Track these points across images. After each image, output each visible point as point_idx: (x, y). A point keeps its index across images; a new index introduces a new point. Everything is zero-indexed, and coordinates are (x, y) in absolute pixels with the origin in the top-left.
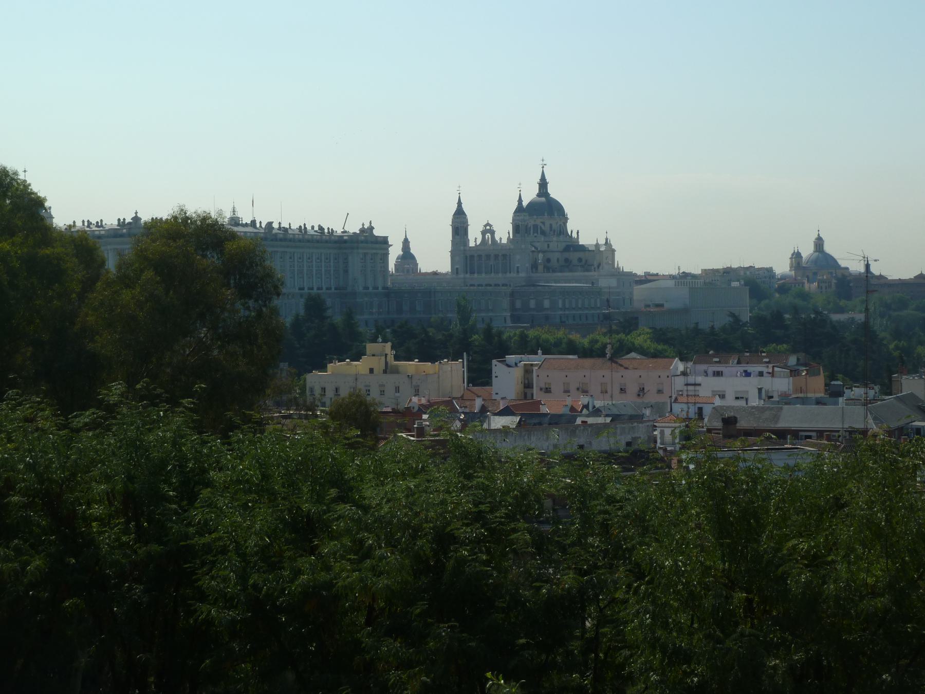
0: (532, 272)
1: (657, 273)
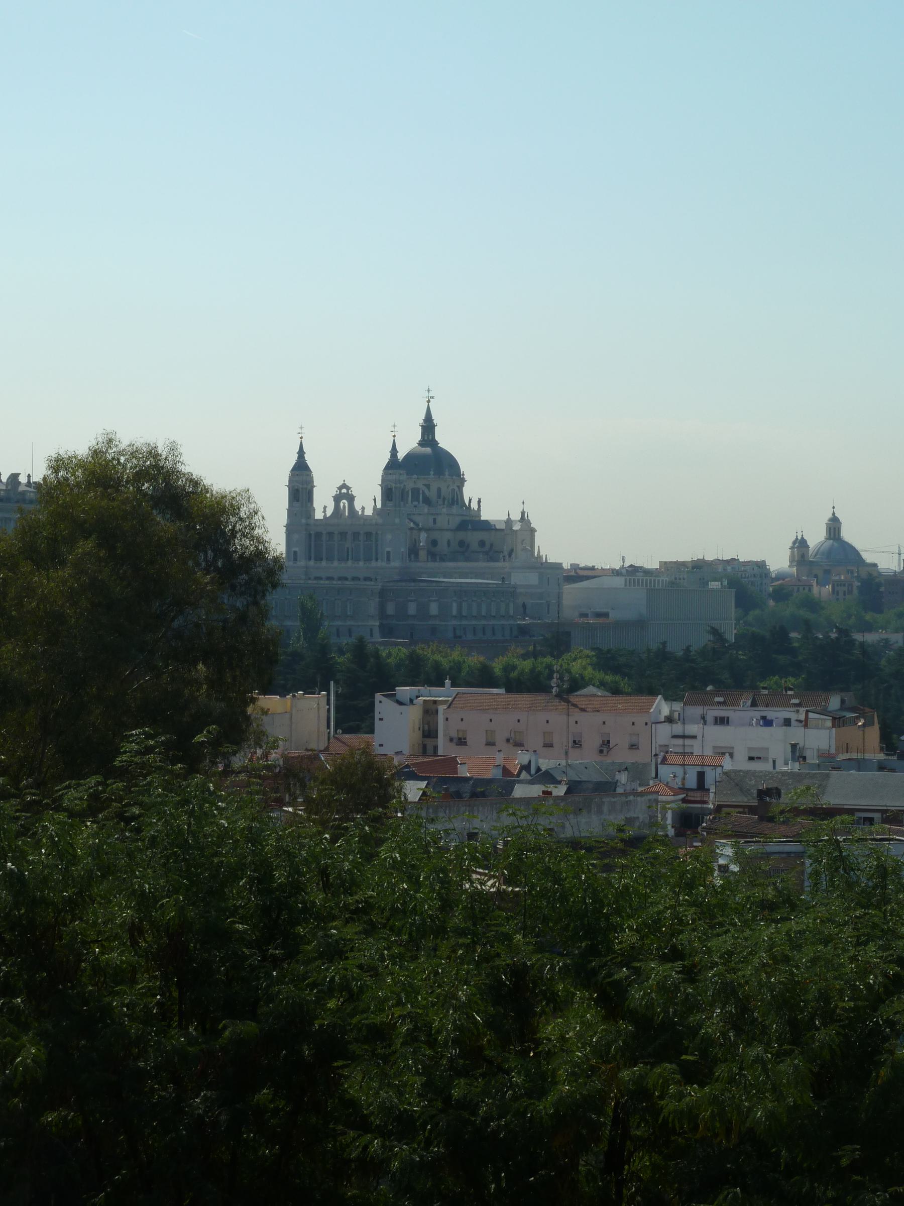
0: (410, 560)
1: (594, 567)
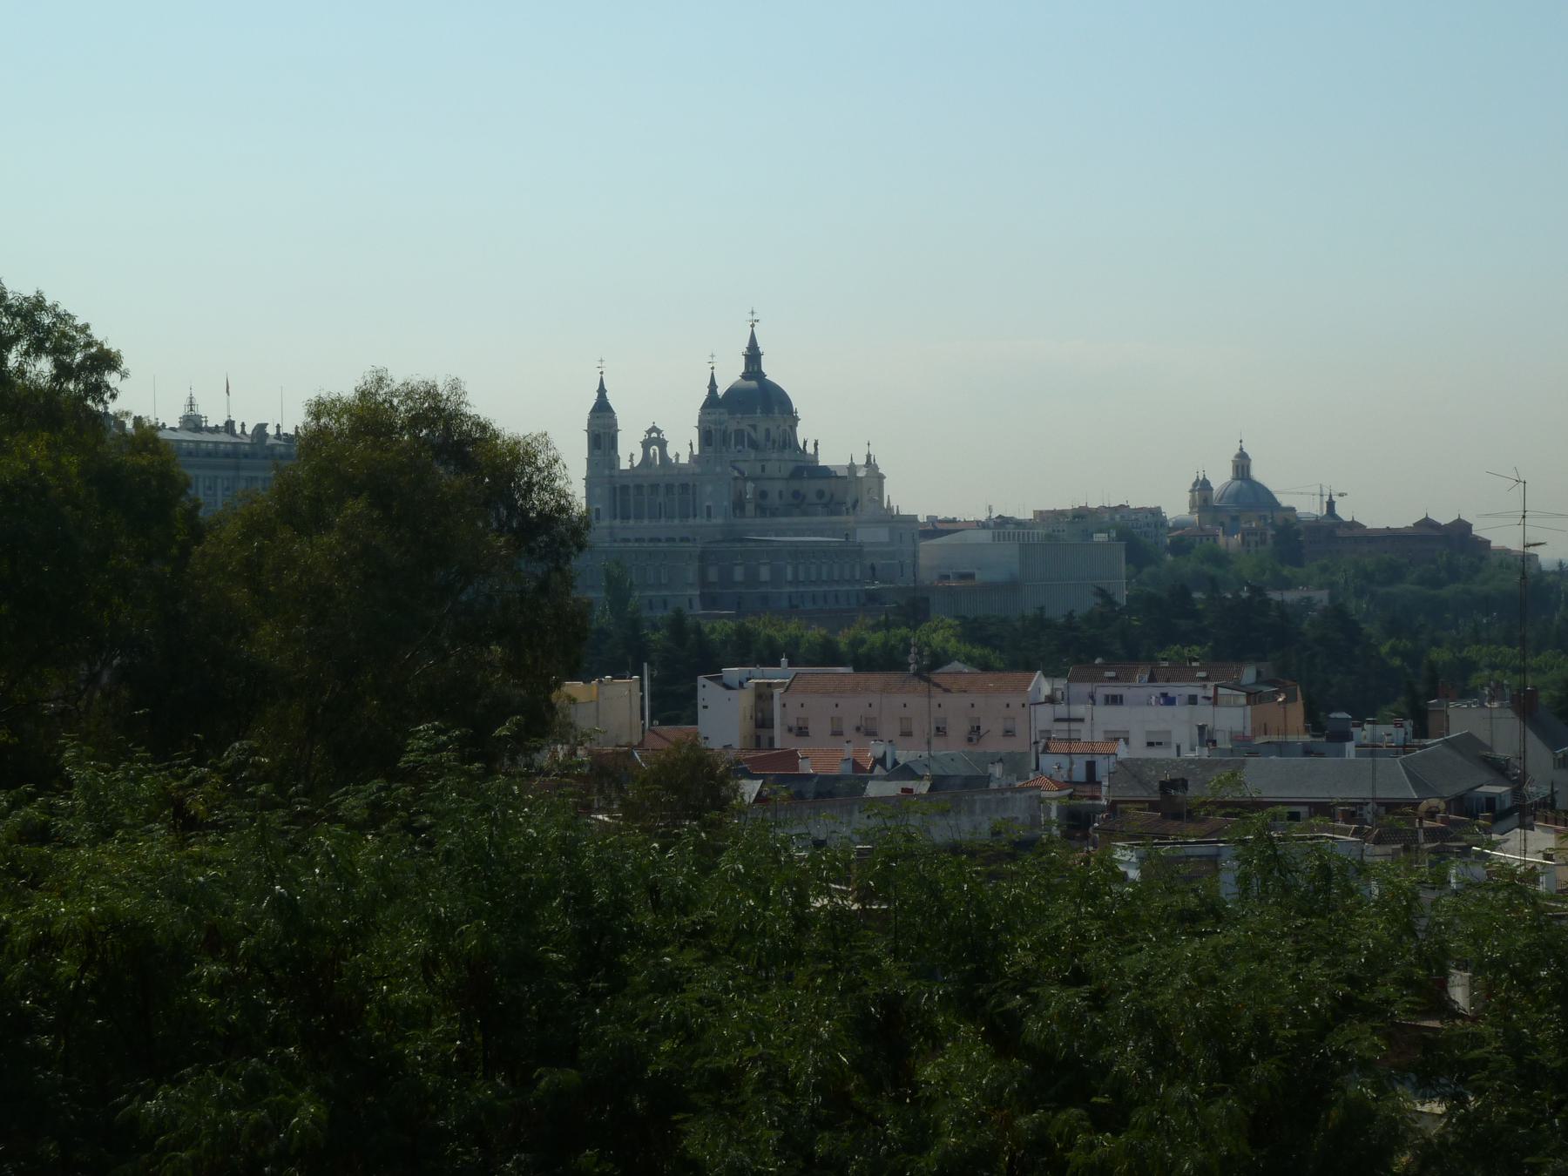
0: (735, 516)
1: (955, 518)
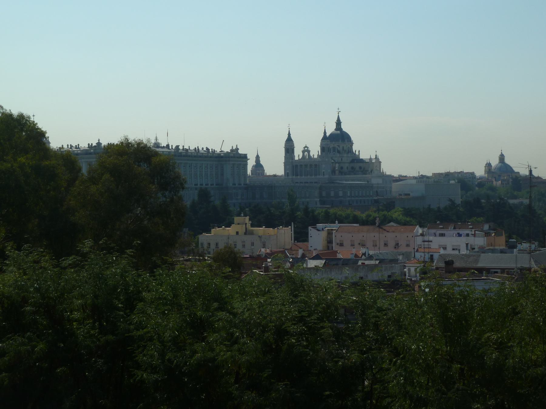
0: (332, 175)
1: (406, 176)
